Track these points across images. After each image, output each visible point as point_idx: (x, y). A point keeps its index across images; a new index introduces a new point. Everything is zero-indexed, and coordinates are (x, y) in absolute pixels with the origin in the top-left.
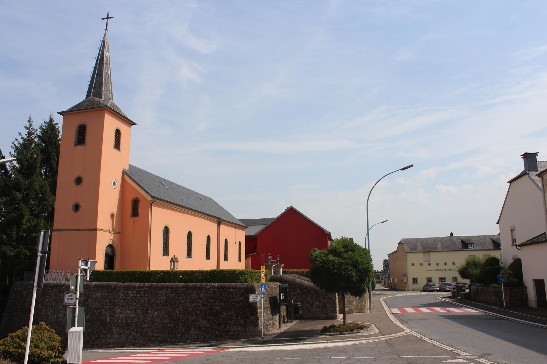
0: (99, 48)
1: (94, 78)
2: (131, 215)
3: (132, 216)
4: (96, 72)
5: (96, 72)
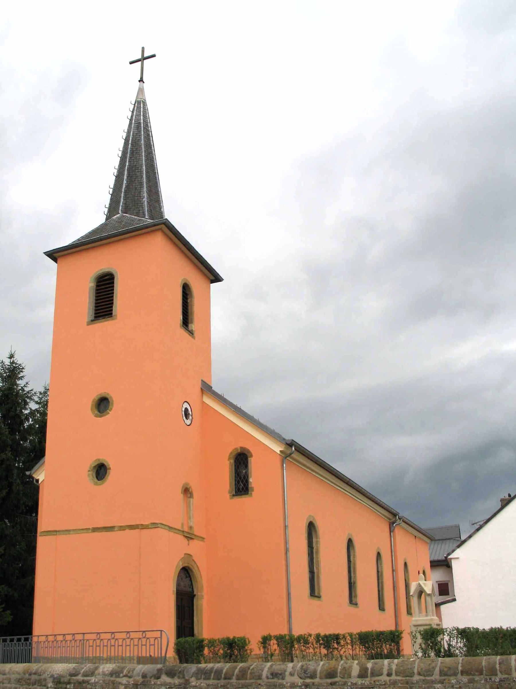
0: (129, 118)
1: (124, 175)
2: (230, 493)
3: (233, 495)
4: (127, 164)
5: (127, 164)
